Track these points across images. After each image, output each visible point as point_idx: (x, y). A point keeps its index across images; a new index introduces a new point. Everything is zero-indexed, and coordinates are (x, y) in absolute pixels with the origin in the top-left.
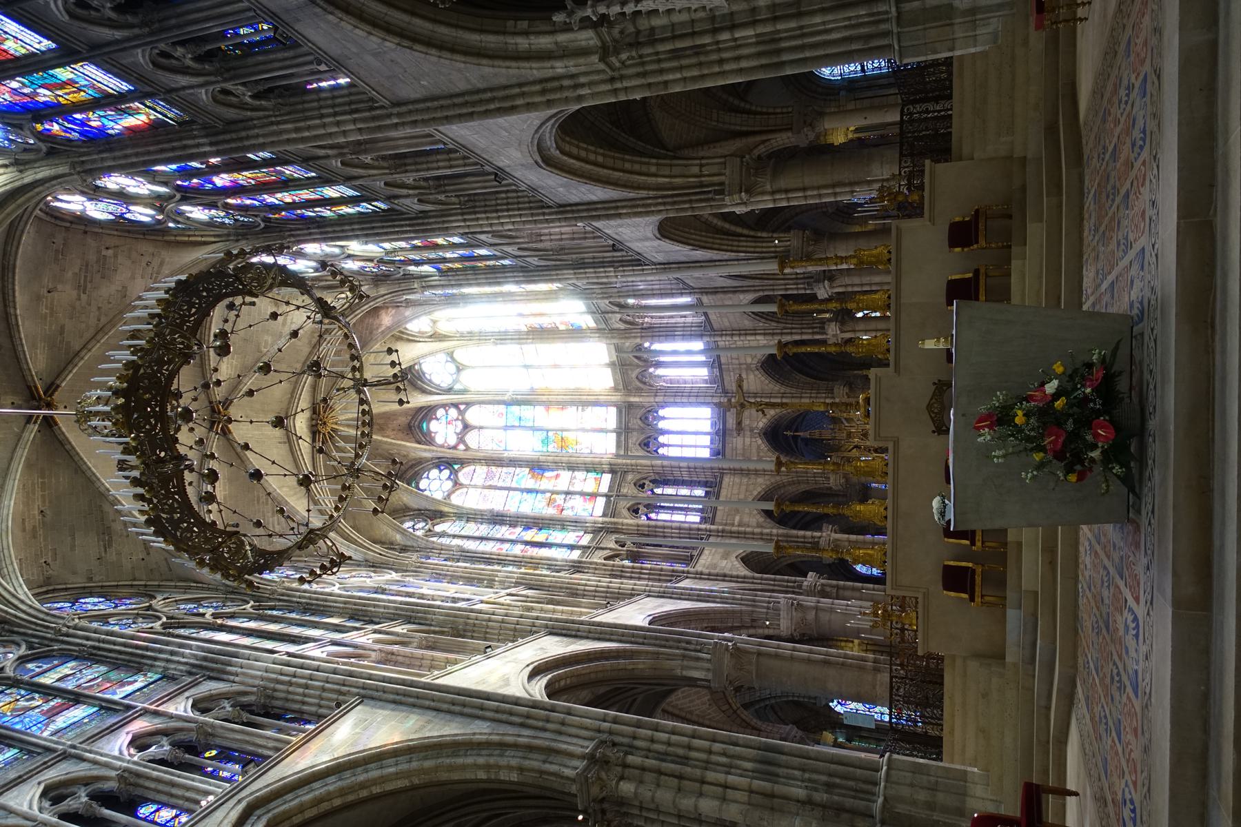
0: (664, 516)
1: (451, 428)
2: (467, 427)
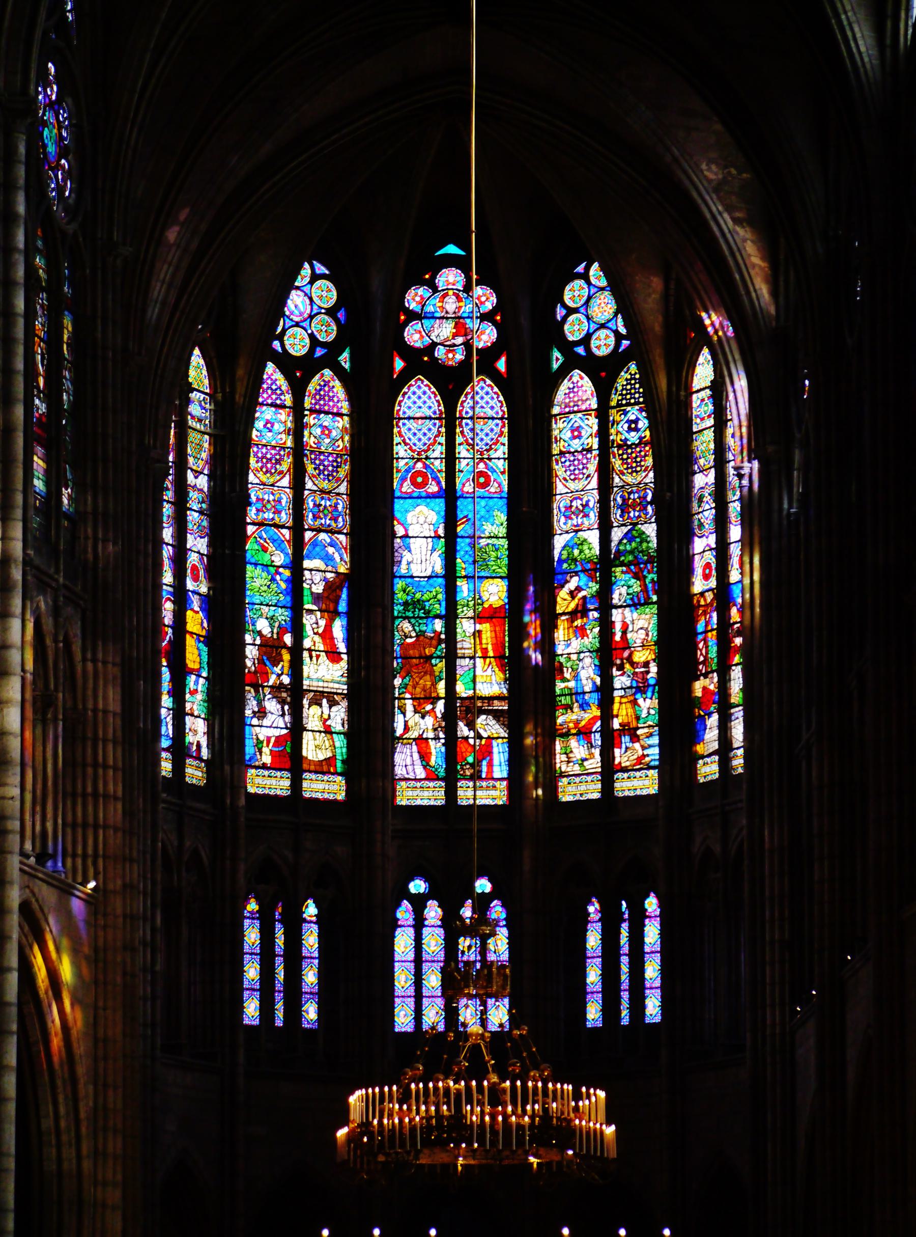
0: (252, 936)
1: (445, 330)
2: (451, 383)
